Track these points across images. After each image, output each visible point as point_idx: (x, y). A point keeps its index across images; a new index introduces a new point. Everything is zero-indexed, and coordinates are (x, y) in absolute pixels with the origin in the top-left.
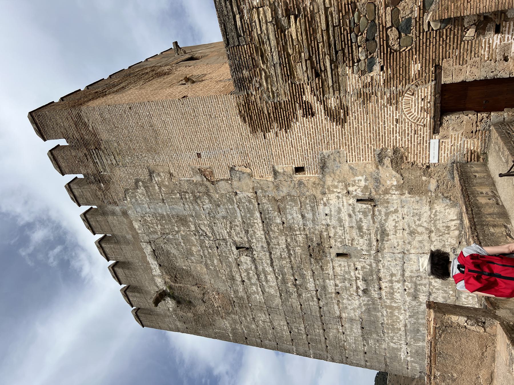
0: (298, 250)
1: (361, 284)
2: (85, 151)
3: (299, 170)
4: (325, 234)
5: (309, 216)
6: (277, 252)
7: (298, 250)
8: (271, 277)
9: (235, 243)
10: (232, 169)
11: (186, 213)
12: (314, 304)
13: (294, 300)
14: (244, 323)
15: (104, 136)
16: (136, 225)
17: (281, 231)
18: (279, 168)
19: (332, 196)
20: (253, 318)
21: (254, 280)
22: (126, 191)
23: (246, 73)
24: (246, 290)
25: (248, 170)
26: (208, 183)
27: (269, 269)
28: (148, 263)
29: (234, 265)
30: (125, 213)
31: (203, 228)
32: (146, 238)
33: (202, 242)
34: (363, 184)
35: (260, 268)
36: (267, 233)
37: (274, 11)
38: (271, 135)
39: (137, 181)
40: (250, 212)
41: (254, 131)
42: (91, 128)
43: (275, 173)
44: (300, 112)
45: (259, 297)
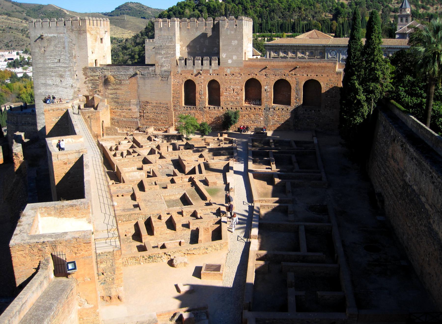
0: (61, 73)
1: (55, 84)
5: (68, 76)
6: (59, 68)
7: (61, 73)
8: (53, 66)
12: (48, 74)
13: (48, 70)
15: (82, 36)
16: (62, 35)
18: (77, 72)
21: (51, 61)
22: (70, 36)
24: (48, 59)
27: (55, 65)
30: (64, 33)
32: (59, 36)
33: (59, 51)
36: (64, 67)
38: (82, 71)
40: (68, 65)
43: (76, 71)
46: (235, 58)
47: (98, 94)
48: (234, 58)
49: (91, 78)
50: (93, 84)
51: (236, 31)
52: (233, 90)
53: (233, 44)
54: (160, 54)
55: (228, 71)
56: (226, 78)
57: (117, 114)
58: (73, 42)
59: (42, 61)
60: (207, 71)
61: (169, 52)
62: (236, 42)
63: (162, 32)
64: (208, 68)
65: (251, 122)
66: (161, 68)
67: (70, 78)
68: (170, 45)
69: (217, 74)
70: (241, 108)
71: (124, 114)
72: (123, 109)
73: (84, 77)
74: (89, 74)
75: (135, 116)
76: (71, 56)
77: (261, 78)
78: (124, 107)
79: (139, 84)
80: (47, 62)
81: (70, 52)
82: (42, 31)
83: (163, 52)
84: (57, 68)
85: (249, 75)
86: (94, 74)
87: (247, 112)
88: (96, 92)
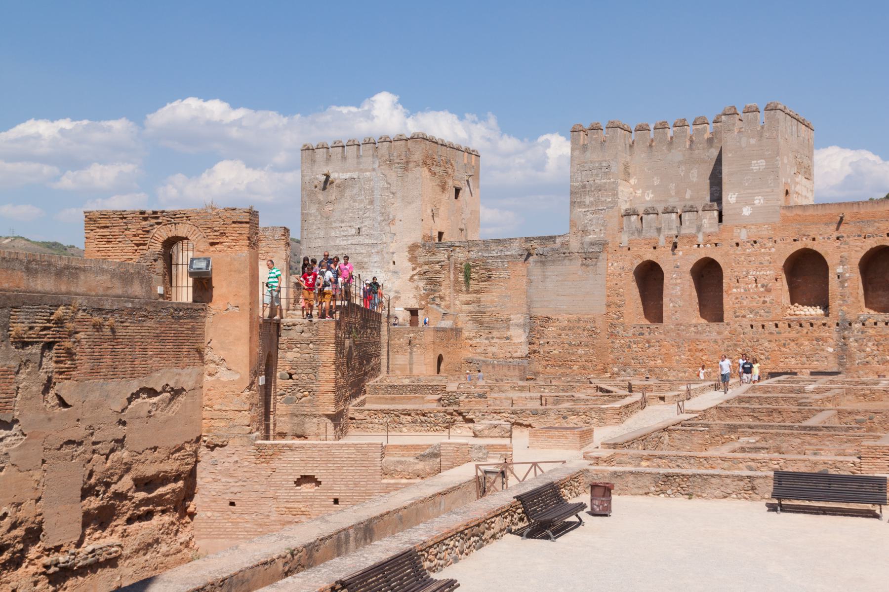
0: (360, 258)
2: (404, 161)
3: (394, 263)
4: (368, 270)
5: (376, 265)
6: (358, 248)
7: (360, 258)
8: (345, 243)
9: (361, 228)
10: (395, 234)
11: (375, 205)
14: (315, 222)
15: (410, 175)
16: (367, 173)
17: (368, 252)
19: (384, 275)
20: (320, 228)
21: (343, 233)
22: (386, 176)
23: (427, 248)
24: (336, 227)
25: (394, 242)
26: (390, 221)
27: (349, 242)
28: (346, 172)
29: (350, 224)
30: (374, 170)
31: (368, 213)
32: (361, 177)
34: (388, 286)
35: (350, 238)
36: (367, 245)
37: (443, 261)
38: (407, 254)
39: (390, 185)
40: (377, 239)
41: (409, 247)
42: (413, 169)
43: (393, 253)
44: (414, 266)
45: (333, 234)
46: (758, 201)
47: (438, 305)
48: (756, 202)
49: (426, 268)
50: (430, 281)
51: (761, 137)
52: (756, 280)
53: (755, 168)
54: (581, 204)
55: (743, 235)
56: (738, 252)
57: (479, 351)
58: (394, 189)
59: (322, 233)
60: (692, 238)
61: (603, 199)
62: (762, 163)
63: (588, 154)
64: (693, 231)
65: (804, 359)
66: (582, 236)
67: (379, 270)
68: (605, 183)
69: (716, 245)
70: (776, 326)
71: (494, 349)
72: (493, 338)
73: (410, 266)
74: (421, 260)
75: (518, 354)
76: (384, 220)
77: (826, 248)
78: (495, 333)
79: (532, 278)
80: (333, 234)
81: (383, 211)
82: (328, 168)
83: (588, 200)
84: (353, 247)
85: (795, 240)
86: (433, 259)
87: (793, 334)
88: (433, 299)
